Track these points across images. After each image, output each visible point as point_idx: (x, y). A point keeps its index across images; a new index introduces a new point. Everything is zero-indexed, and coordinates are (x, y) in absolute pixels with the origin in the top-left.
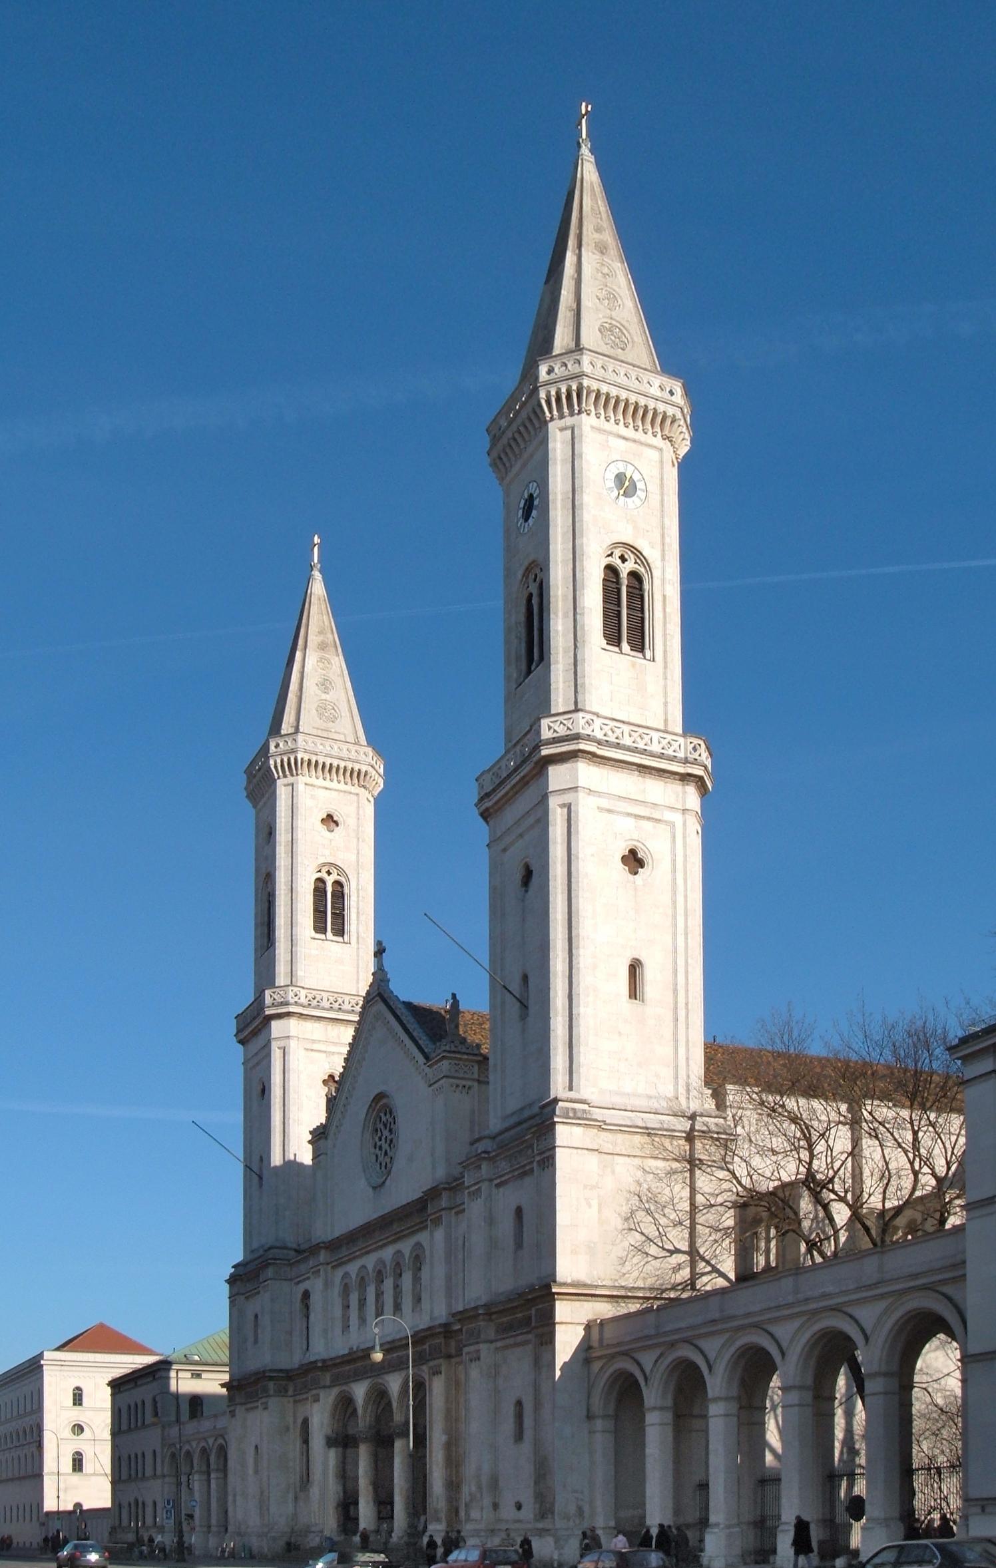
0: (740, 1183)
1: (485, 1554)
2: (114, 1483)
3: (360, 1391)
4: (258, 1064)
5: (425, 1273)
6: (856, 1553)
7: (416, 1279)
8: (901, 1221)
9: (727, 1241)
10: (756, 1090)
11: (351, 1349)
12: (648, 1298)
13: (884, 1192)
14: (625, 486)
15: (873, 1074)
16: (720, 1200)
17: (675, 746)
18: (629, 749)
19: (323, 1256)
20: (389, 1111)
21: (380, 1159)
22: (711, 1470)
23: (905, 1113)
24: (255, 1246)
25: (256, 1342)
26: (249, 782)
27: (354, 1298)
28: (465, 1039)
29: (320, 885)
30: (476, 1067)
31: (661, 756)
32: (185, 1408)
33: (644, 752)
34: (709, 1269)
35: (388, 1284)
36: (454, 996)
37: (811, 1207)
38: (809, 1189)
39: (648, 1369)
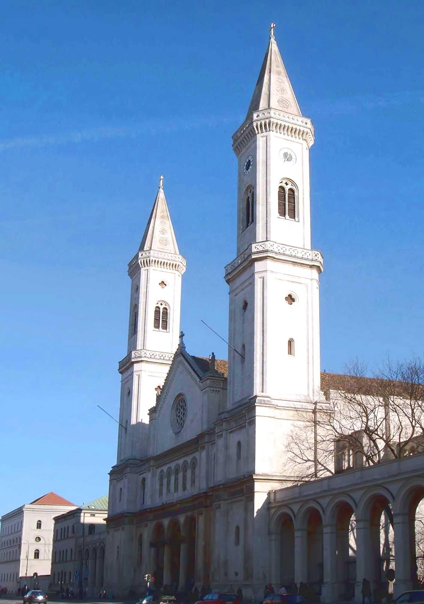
0: (336, 431)
1: (220, 596)
2: (52, 564)
3: (166, 522)
4: (127, 382)
5: (197, 471)
6: (391, 595)
7: (193, 473)
8: (408, 447)
9: (331, 456)
10: (343, 392)
11: (163, 503)
12: (296, 481)
13: (400, 435)
14: (287, 157)
15: (393, 385)
16: (328, 438)
17: (308, 254)
19: (152, 463)
20: (184, 401)
21: (179, 421)
22: (324, 558)
23: (408, 402)
24: (122, 458)
25: (120, 500)
26: (130, 269)
27: (165, 481)
28: (217, 371)
29: (158, 309)
30: (222, 383)
32: (87, 530)
33: (295, 257)
34: (323, 468)
35: (181, 475)
36: (213, 353)
37: (368, 441)
38: (367, 433)
39: (296, 512)
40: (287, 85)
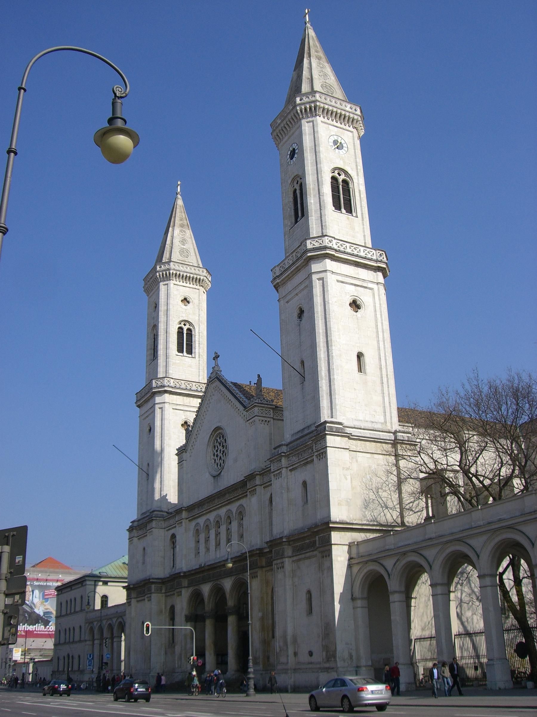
14: (338, 145)
31: (365, 258)
40: (328, 69)
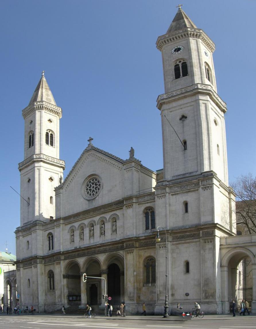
18: (50, 161)
